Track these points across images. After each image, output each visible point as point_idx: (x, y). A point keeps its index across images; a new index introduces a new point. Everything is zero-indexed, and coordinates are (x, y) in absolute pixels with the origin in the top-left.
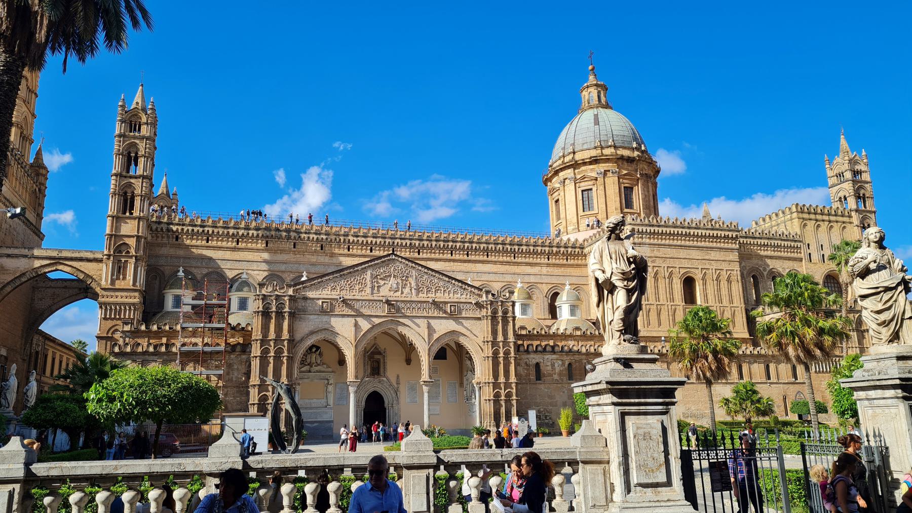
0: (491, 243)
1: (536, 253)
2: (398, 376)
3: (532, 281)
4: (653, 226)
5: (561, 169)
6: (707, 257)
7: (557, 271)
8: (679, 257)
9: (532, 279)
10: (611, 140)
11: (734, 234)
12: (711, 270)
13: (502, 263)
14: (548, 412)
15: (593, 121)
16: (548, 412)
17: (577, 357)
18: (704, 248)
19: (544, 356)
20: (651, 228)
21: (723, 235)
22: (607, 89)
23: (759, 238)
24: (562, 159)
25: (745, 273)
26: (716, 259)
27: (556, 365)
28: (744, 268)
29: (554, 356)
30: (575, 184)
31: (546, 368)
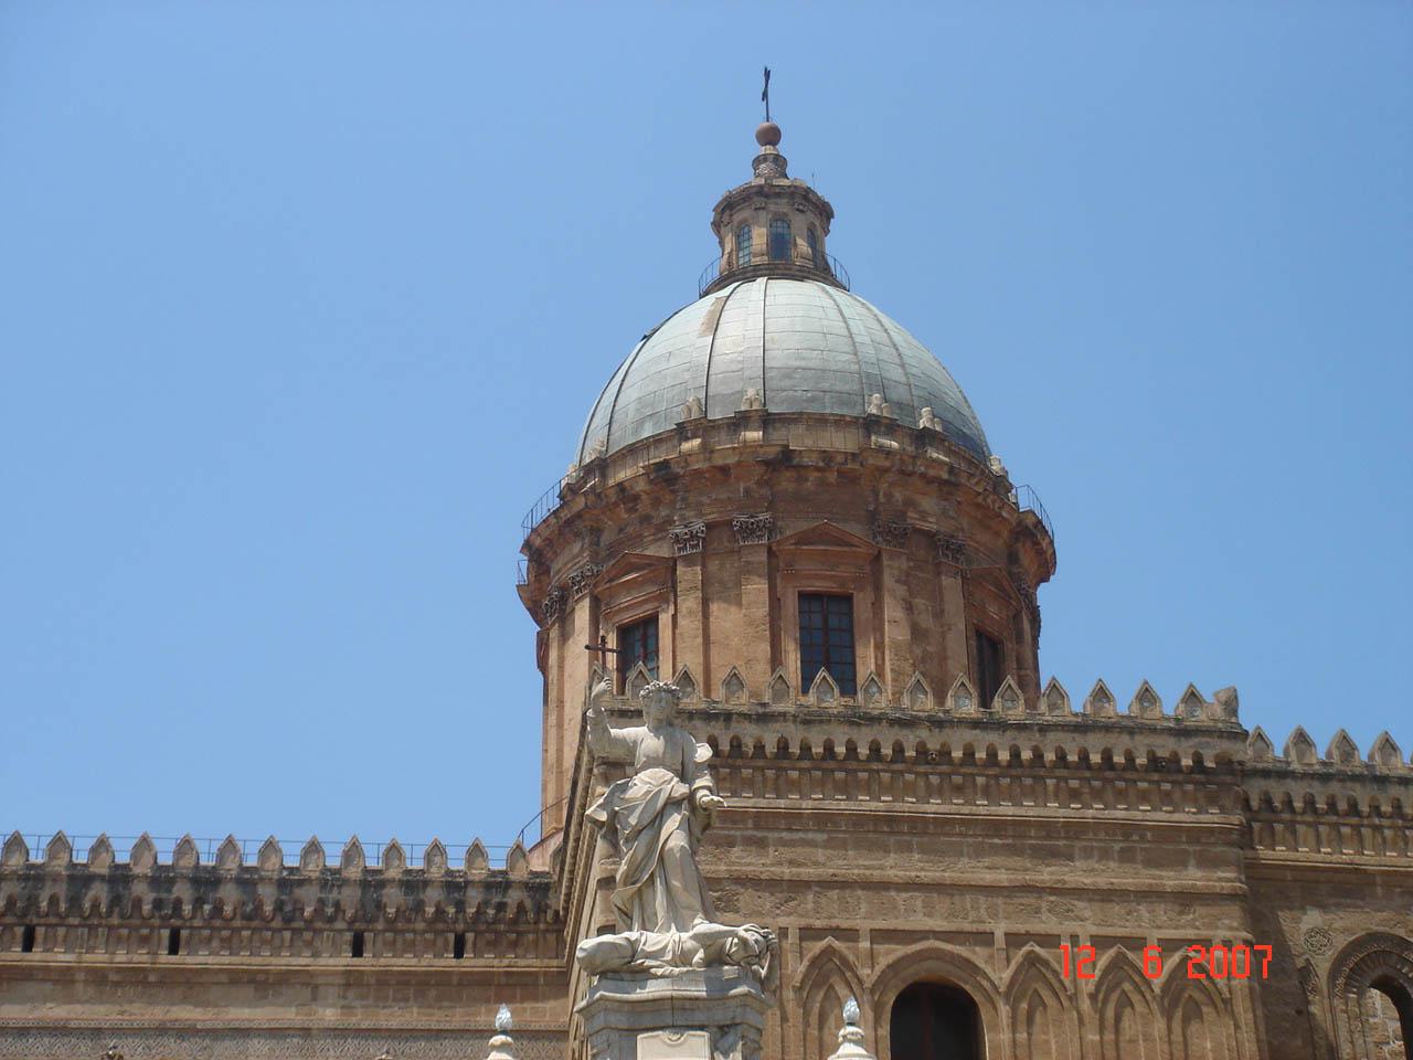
1: (288, 914)
8: (877, 875)
22: (825, 212)
25: (1323, 965)
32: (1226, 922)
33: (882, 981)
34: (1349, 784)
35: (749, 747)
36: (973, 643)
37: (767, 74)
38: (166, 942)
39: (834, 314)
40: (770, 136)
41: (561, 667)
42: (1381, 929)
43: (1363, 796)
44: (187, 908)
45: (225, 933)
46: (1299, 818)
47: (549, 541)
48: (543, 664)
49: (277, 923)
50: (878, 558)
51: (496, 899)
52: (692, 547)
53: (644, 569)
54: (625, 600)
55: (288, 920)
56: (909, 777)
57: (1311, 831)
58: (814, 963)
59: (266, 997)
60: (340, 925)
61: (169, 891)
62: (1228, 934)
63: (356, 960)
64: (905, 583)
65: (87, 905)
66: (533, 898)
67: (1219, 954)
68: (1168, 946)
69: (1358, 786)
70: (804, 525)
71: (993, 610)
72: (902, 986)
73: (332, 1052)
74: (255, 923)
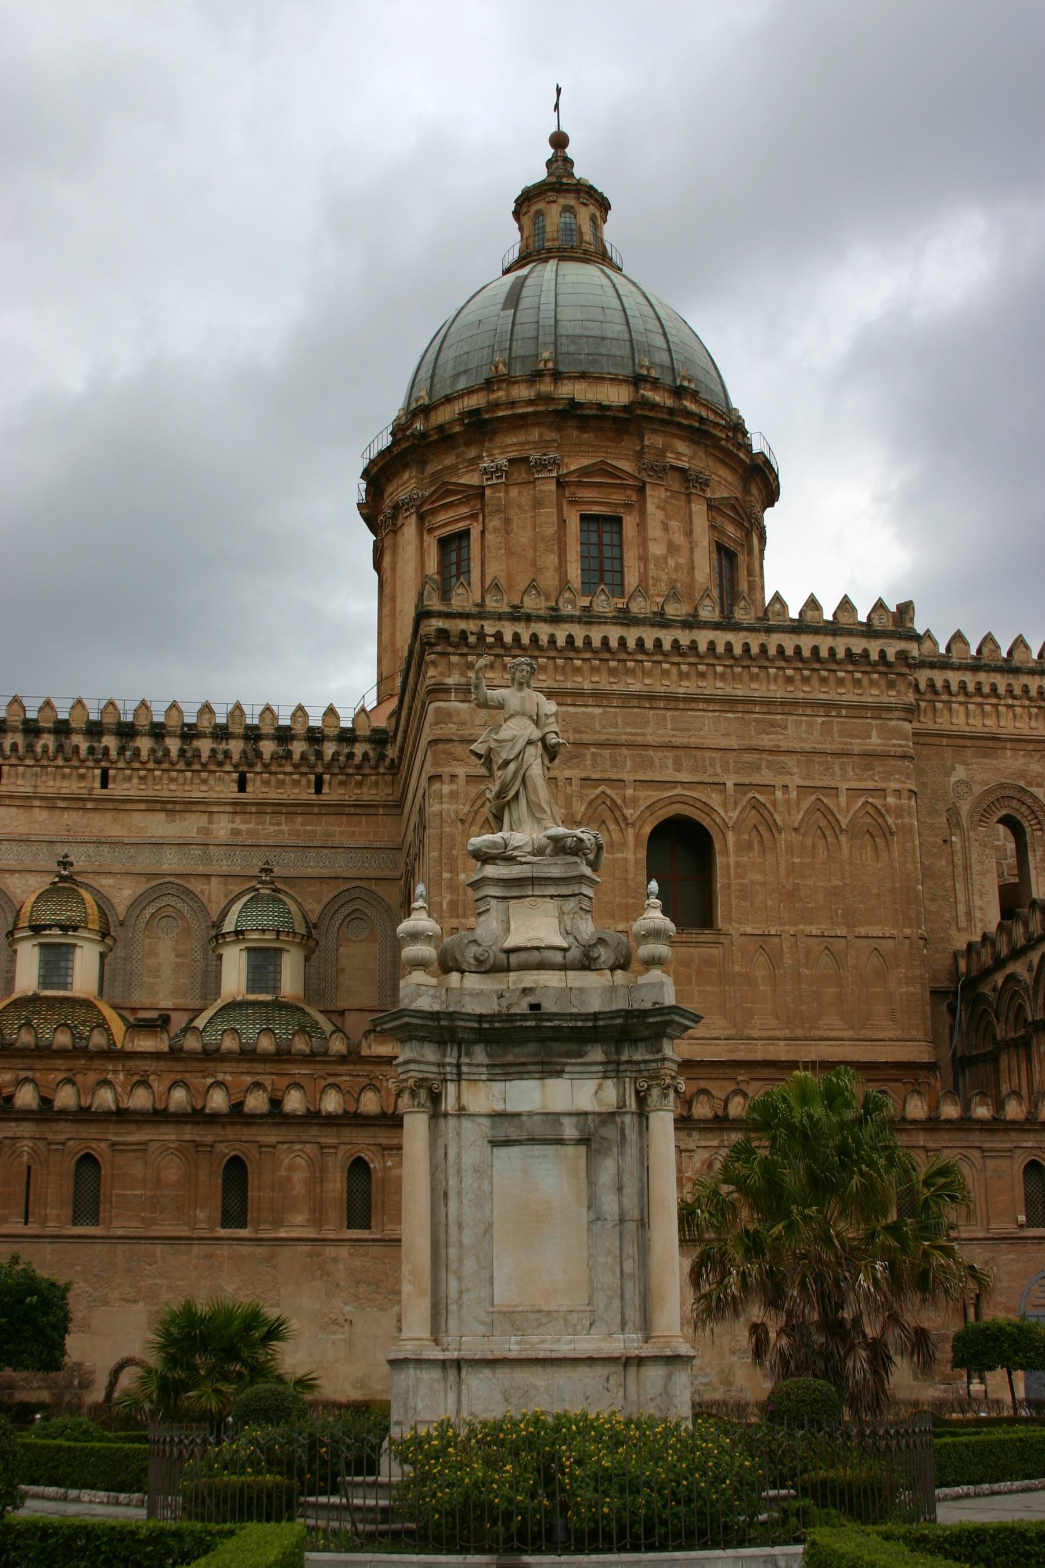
0: (14, 730)
1: (189, 759)
3: (166, 868)
4: (528, 618)
6: (766, 741)
7: (270, 829)
8: (640, 740)
9: (170, 862)
11: (892, 648)
12: (779, 794)
13: (50, 803)
20: (520, 628)
21: (841, 654)
22: (604, 205)
25: (965, 808)
26: (807, 747)
28: (962, 789)
30: (421, 518)
32: (897, 776)
33: (641, 819)
34: (992, 674)
35: (544, 640)
36: (715, 556)
37: (559, 91)
39: (611, 291)
40: (559, 141)
41: (394, 570)
42: (1008, 781)
43: (1001, 681)
44: (113, 753)
45: (142, 773)
46: (954, 699)
47: (382, 470)
48: (378, 565)
49: (181, 766)
50: (641, 490)
51: (346, 750)
52: (498, 478)
53: (458, 494)
54: (442, 517)
55: (189, 764)
56: (666, 666)
57: (962, 709)
58: (590, 803)
59: (174, 821)
61: (99, 741)
62: (897, 786)
63: (241, 795)
64: (663, 509)
65: (39, 749)
66: (375, 749)
67: (890, 800)
68: (854, 792)
69: (998, 676)
70: (585, 462)
71: (730, 529)
72: (657, 823)
73: (225, 862)
74: (165, 766)
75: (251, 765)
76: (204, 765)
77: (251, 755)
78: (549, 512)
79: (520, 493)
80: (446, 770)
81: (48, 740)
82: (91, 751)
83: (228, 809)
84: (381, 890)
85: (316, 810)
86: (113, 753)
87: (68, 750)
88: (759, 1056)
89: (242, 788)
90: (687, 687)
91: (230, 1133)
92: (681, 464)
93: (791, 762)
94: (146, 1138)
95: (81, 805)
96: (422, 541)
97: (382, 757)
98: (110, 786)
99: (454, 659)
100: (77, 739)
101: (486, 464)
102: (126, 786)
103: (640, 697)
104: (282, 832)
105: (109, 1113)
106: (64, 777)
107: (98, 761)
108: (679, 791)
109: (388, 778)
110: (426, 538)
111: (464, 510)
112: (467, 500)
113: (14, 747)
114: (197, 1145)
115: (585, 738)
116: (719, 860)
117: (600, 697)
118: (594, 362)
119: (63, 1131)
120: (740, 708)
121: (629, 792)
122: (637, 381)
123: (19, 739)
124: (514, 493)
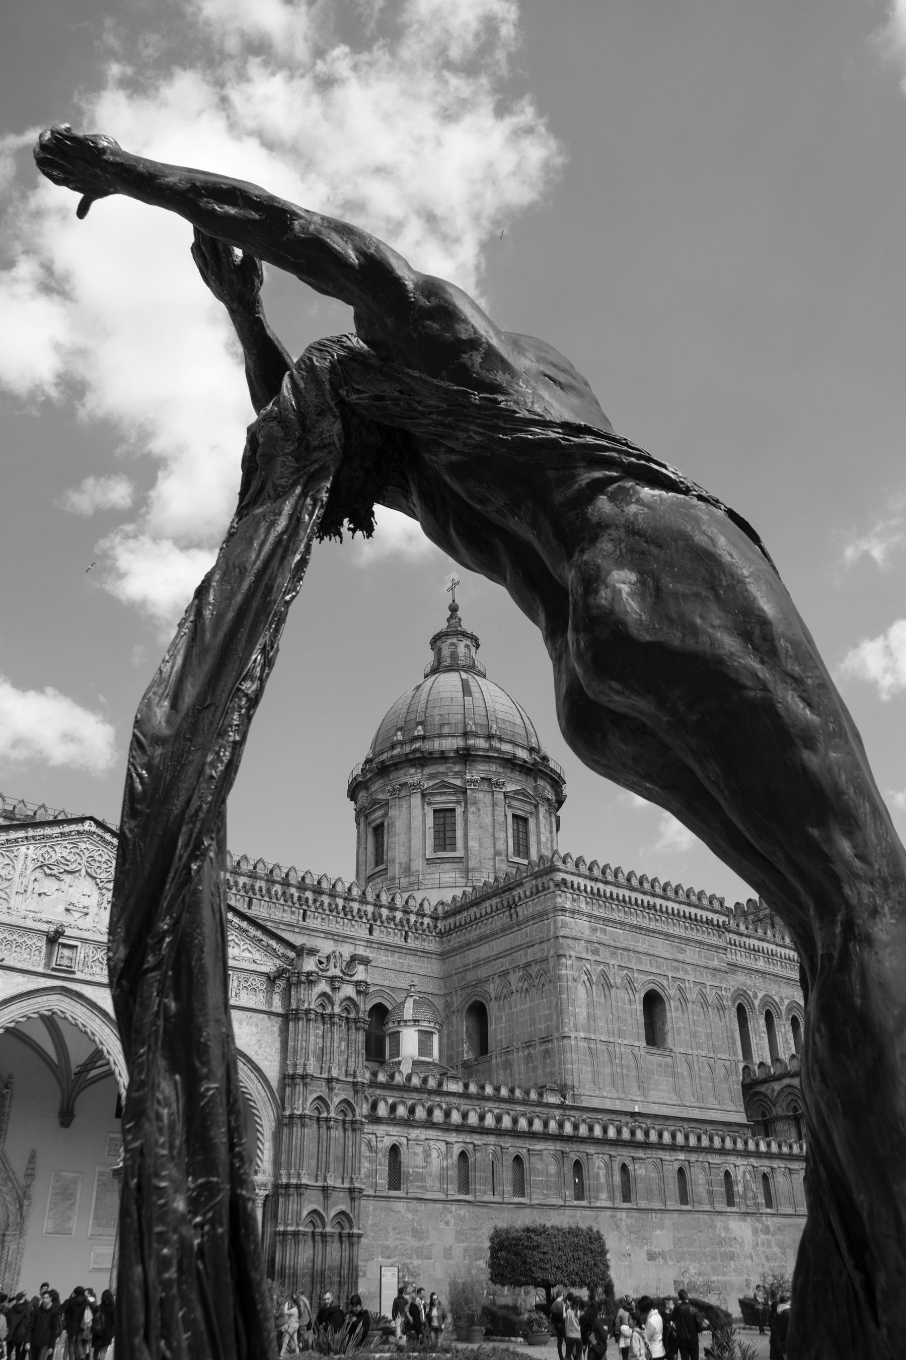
0: (261, 879)
2: (32, 1158)
5: (395, 764)
6: (680, 957)
8: (637, 949)
10: (494, 726)
14: (411, 1274)
15: (460, 689)
16: (411, 1274)
17: (478, 1140)
18: (676, 937)
19: (411, 1131)
20: (593, 884)
22: (477, 646)
23: (747, 936)
24: (397, 751)
26: (694, 962)
27: (434, 1154)
29: (431, 1134)
30: (423, 795)
31: (412, 1160)
38: (301, 916)
40: (454, 609)
44: (311, 901)
49: (342, 915)
50: (536, 806)
51: (420, 921)
54: (438, 799)
60: (364, 920)
63: (371, 937)
67: (724, 992)
74: (334, 914)
75: (375, 921)
76: (353, 916)
77: (377, 915)
78: (500, 810)
79: (484, 796)
80: (567, 953)
81: (278, 888)
82: (300, 898)
83: (364, 944)
84: (434, 1000)
85: (404, 951)
86: (311, 901)
87: (288, 895)
88: (690, 1116)
89: (371, 933)
90: (652, 925)
91: (575, 1147)
92: (549, 797)
93: (689, 968)
94: (542, 1147)
95: (292, 929)
96: (423, 809)
97: (436, 927)
98: (307, 920)
99: (568, 895)
100: (293, 890)
101: (468, 777)
102: (315, 922)
103: (637, 927)
104: (388, 961)
105: (524, 1132)
106: (284, 911)
107: (301, 905)
108: (652, 977)
109: (437, 939)
110: (426, 807)
111: (453, 798)
112: (455, 793)
113: (261, 889)
114: (563, 1152)
115: (619, 945)
116: (668, 1014)
117: (622, 924)
118: (513, 736)
119: (507, 1142)
120: (671, 939)
121: (635, 975)
122: (531, 750)
123: (263, 884)
124: (481, 795)
